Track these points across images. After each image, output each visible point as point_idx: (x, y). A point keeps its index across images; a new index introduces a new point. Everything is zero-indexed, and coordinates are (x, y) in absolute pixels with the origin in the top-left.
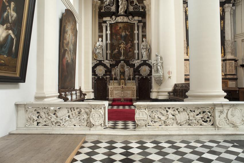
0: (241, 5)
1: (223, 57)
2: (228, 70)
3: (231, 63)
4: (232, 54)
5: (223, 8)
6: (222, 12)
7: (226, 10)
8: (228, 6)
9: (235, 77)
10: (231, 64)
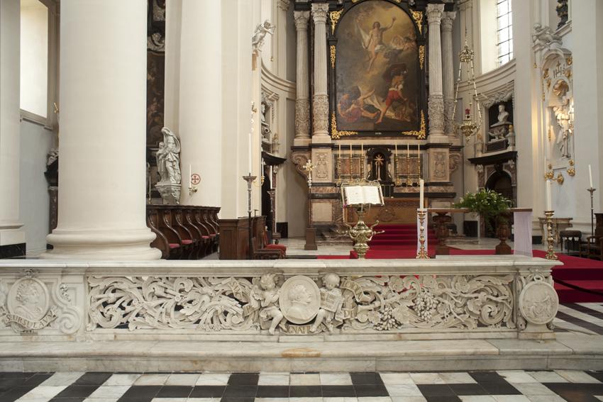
0: (472, 7)
1: (423, 139)
2: (432, 174)
3: (442, 153)
4: (446, 132)
5: (424, 14)
6: (421, 23)
7: (430, 20)
8: (433, 9)
9: (450, 190)
10: (440, 157)
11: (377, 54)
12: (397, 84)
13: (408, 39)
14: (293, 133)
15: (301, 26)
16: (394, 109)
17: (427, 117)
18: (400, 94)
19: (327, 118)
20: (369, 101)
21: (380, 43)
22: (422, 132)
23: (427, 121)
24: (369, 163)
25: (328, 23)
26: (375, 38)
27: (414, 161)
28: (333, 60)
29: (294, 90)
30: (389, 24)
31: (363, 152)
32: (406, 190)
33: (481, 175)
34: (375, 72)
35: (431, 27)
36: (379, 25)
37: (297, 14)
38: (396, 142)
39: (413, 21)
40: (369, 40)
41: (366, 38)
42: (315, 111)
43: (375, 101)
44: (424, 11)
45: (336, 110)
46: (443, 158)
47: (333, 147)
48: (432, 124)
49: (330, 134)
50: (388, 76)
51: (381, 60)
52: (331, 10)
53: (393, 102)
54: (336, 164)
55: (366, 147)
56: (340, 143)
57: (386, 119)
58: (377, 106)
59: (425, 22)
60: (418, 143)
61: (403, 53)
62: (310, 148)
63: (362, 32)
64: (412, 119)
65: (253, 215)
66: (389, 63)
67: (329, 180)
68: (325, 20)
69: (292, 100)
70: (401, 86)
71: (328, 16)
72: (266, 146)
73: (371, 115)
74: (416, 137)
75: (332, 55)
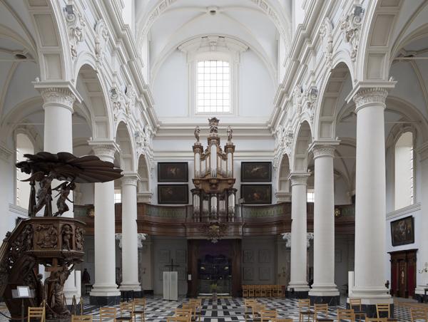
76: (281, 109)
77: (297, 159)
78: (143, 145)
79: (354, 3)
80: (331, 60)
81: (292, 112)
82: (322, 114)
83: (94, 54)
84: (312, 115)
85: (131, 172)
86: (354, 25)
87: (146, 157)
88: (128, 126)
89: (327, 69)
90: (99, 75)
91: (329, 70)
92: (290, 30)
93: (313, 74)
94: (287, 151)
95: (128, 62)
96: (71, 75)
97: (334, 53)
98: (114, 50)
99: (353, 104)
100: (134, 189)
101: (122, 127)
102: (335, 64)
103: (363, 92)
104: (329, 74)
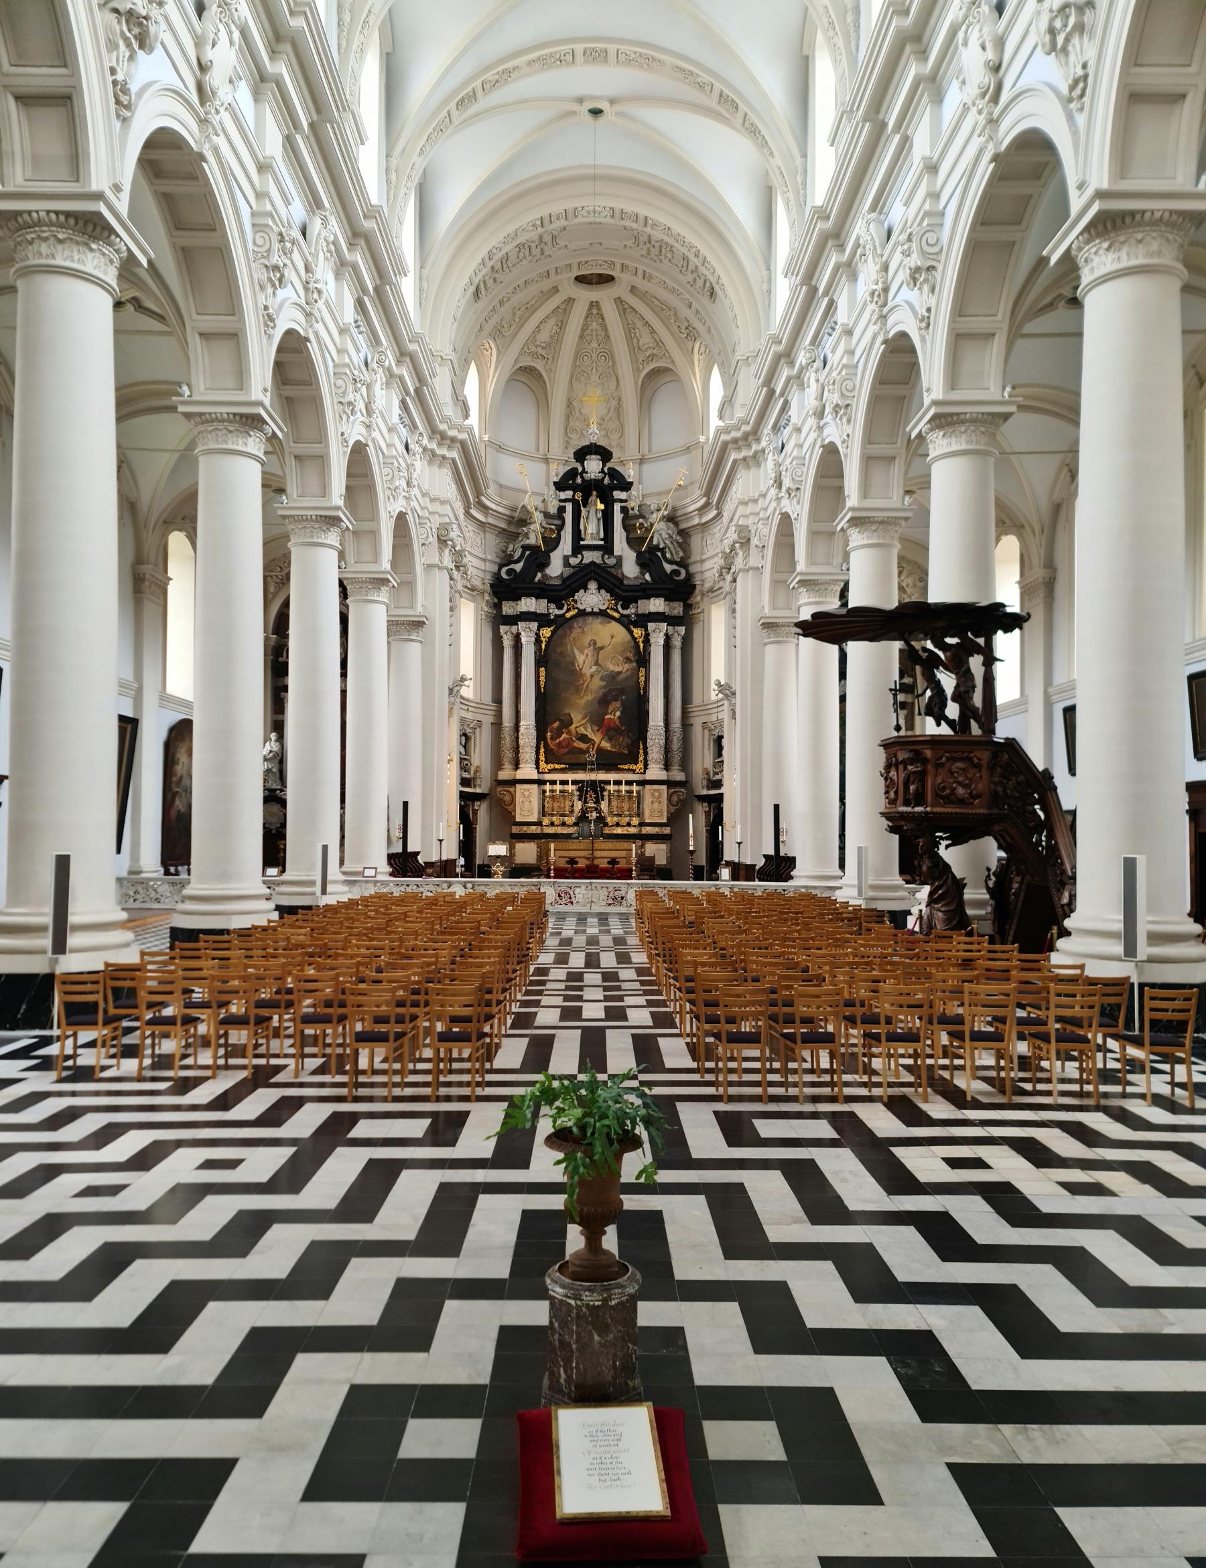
7: (652, 640)
11: (592, 676)
12: (614, 711)
13: (628, 660)
14: (498, 765)
15: (507, 642)
16: (610, 740)
17: (645, 748)
18: (617, 722)
19: (534, 750)
20: (582, 731)
21: (597, 663)
22: (641, 765)
23: (646, 754)
24: (580, 799)
25: (538, 641)
26: (590, 658)
27: (630, 798)
28: (542, 684)
29: (499, 714)
30: (606, 641)
31: (570, 788)
32: (619, 831)
33: (707, 814)
34: (589, 697)
35: (653, 648)
36: (595, 643)
37: (503, 629)
38: (612, 777)
39: (634, 639)
40: (583, 660)
41: (580, 658)
42: (521, 742)
43: (589, 730)
44: (646, 630)
45: (545, 739)
46: (660, 796)
47: (540, 782)
48: (650, 758)
49: (538, 767)
50: (604, 701)
51: (597, 683)
52: (539, 629)
53: (610, 732)
54: (544, 800)
55: (574, 782)
56: (548, 777)
57: (600, 751)
58: (591, 735)
59: (647, 641)
60: (631, 777)
61: (622, 676)
62: (514, 782)
63: (576, 652)
64: (630, 751)
65: (444, 858)
66: (604, 687)
67: (535, 819)
68: (533, 639)
69: (497, 725)
70: (618, 714)
71: (537, 635)
72: (465, 782)
73: (583, 746)
74: (634, 771)
75: (542, 679)
76: (816, 289)
77: (868, 461)
78: (361, 406)
79: (927, 207)
80: (993, 122)
81: (852, 302)
82: (960, 309)
83: (194, 98)
84: (923, 313)
85: (322, 503)
86: (924, 254)
87: (371, 450)
88: (313, 347)
89: (981, 152)
90: (211, 169)
91: (988, 156)
92: (850, 18)
93: (932, 168)
94: (834, 433)
95: (312, 125)
96: (112, 168)
97: (1005, 97)
98: (261, 81)
99: (1070, 264)
100: (329, 559)
101: (293, 357)
102: (1008, 132)
103: (1110, 224)
104: (985, 169)
